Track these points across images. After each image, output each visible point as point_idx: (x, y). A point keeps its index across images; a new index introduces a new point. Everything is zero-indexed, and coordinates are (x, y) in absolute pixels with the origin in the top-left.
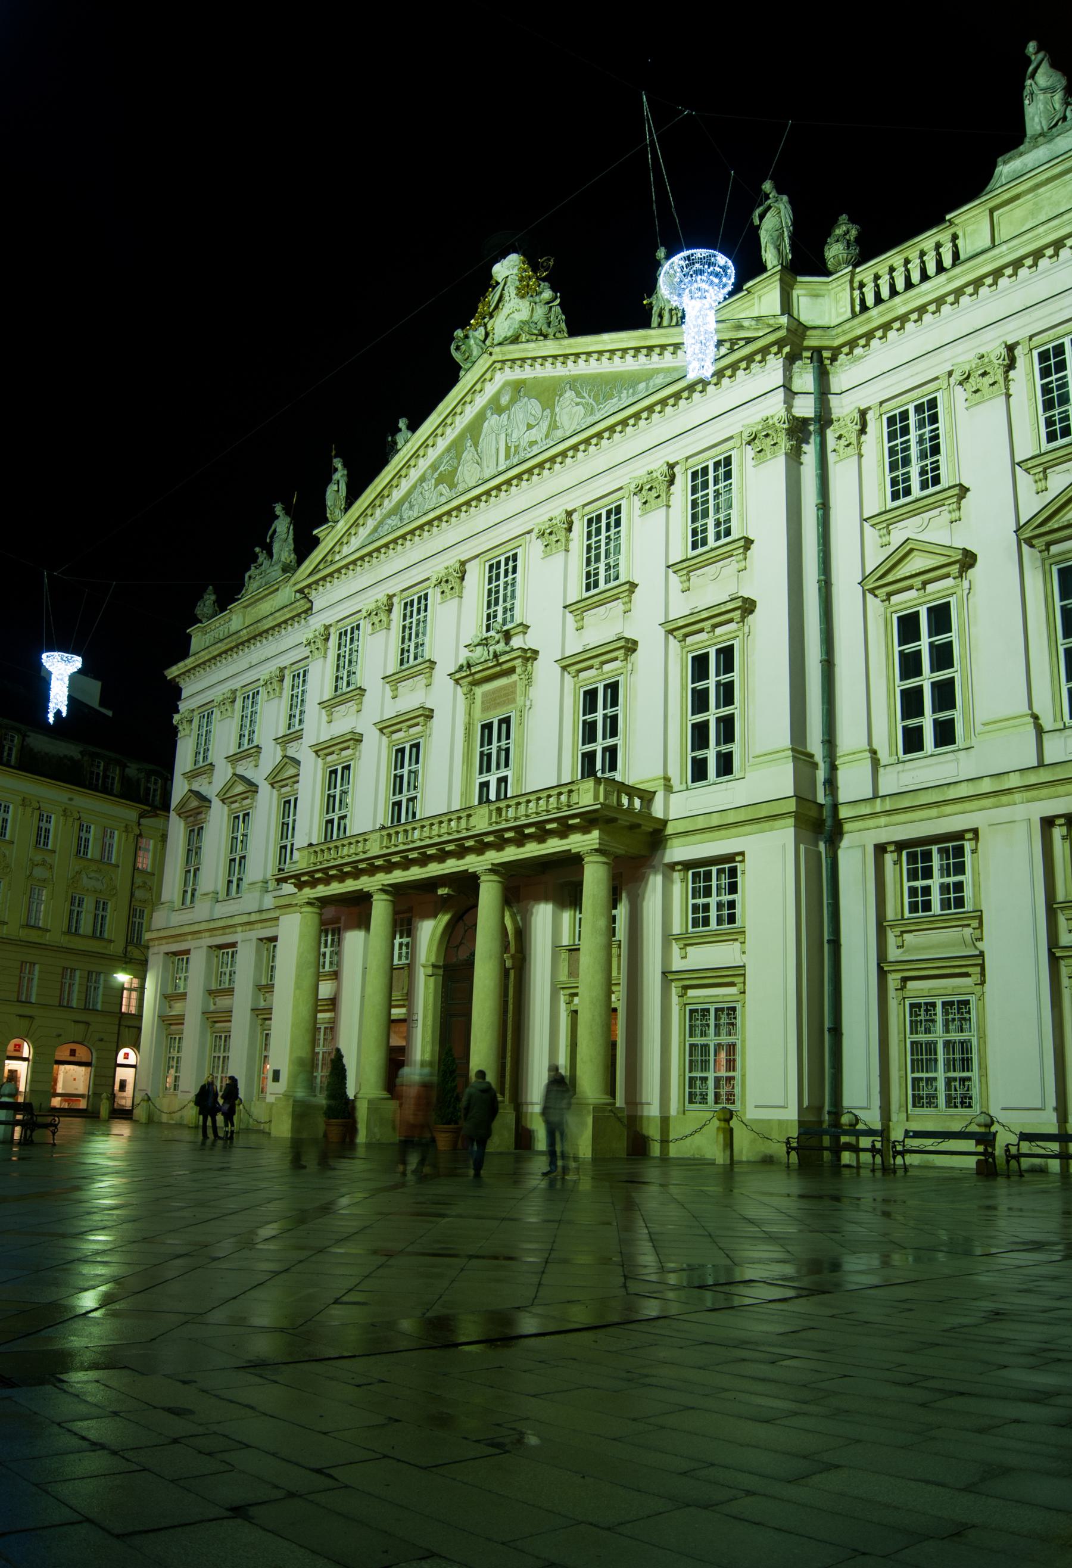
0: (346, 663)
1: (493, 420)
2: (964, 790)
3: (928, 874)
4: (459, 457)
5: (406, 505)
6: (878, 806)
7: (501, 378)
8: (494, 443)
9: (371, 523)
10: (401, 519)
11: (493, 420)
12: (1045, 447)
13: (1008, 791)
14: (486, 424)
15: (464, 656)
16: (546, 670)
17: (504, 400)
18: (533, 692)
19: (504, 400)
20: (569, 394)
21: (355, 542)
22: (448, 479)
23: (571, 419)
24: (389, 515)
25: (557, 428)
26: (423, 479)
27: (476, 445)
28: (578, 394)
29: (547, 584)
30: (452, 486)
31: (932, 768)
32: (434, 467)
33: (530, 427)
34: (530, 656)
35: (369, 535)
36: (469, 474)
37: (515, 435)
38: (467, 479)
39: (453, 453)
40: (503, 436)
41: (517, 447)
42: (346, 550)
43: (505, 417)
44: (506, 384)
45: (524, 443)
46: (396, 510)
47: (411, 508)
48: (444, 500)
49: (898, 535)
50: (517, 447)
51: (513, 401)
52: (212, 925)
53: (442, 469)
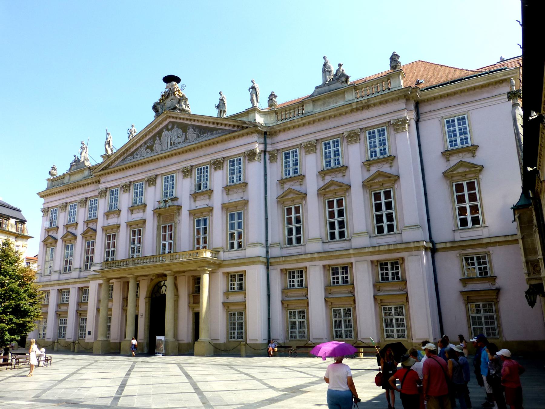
0: (114, 201)
1: (165, 133)
2: (303, 257)
3: (294, 277)
4: (154, 142)
5: (135, 153)
7: (168, 120)
9: (122, 158)
10: (134, 158)
11: (165, 133)
12: (325, 168)
13: (315, 258)
14: (163, 133)
15: (157, 206)
16: (185, 212)
17: (170, 127)
18: (180, 218)
19: (170, 127)
20: (191, 130)
21: (117, 162)
22: (151, 148)
23: (192, 138)
24: (129, 156)
25: (187, 139)
26: (141, 146)
27: (160, 139)
28: (194, 131)
29: (184, 187)
30: (152, 150)
31: (295, 250)
32: (145, 143)
33: (178, 137)
34: (179, 208)
36: (157, 147)
38: (157, 149)
39: (152, 140)
41: (174, 143)
42: (113, 165)
43: (170, 132)
44: (170, 122)
45: (176, 142)
46: (132, 154)
47: (137, 155)
48: (149, 155)
49: (287, 186)
50: (174, 143)
51: (173, 128)
52: (59, 282)
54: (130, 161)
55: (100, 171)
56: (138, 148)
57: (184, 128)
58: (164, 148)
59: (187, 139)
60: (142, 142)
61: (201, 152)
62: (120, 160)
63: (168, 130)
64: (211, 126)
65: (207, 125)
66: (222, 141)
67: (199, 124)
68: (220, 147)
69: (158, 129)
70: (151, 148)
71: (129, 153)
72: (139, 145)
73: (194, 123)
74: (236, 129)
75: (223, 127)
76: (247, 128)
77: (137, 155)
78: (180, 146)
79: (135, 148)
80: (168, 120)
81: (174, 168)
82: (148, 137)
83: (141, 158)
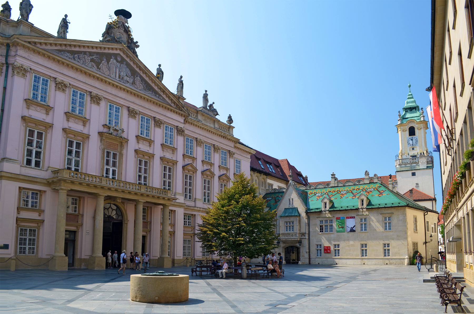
5: (76, 55)
6: (196, 209)
8: (115, 69)
11: (113, 61)
14: (112, 60)
17: (119, 59)
20: (139, 78)
21: (49, 47)
22: (98, 65)
26: (85, 53)
30: (98, 68)
32: (91, 54)
33: (127, 76)
35: (56, 50)
37: (122, 73)
40: (118, 70)
42: (44, 47)
44: (119, 54)
46: (73, 53)
53: (93, 57)
54: (66, 58)
55: (29, 43)
56: (81, 52)
57: (134, 73)
58: (112, 76)
59: (135, 84)
60: (87, 50)
61: (147, 105)
62: (54, 48)
63: (117, 61)
64: (156, 88)
65: (153, 85)
66: (165, 108)
67: (147, 79)
68: (160, 110)
69: (106, 51)
70: (98, 65)
71: (68, 48)
72: (82, 49)
73: (144, 76)
74: (173, 105)
75: (164, 96)
76: (181, 111)
77: (79, 58)
78: (128, 85)
79: (77, 49)
80: (118, 52)
81: (122, 102)
82: (95, 50)
83: (83, 66)
